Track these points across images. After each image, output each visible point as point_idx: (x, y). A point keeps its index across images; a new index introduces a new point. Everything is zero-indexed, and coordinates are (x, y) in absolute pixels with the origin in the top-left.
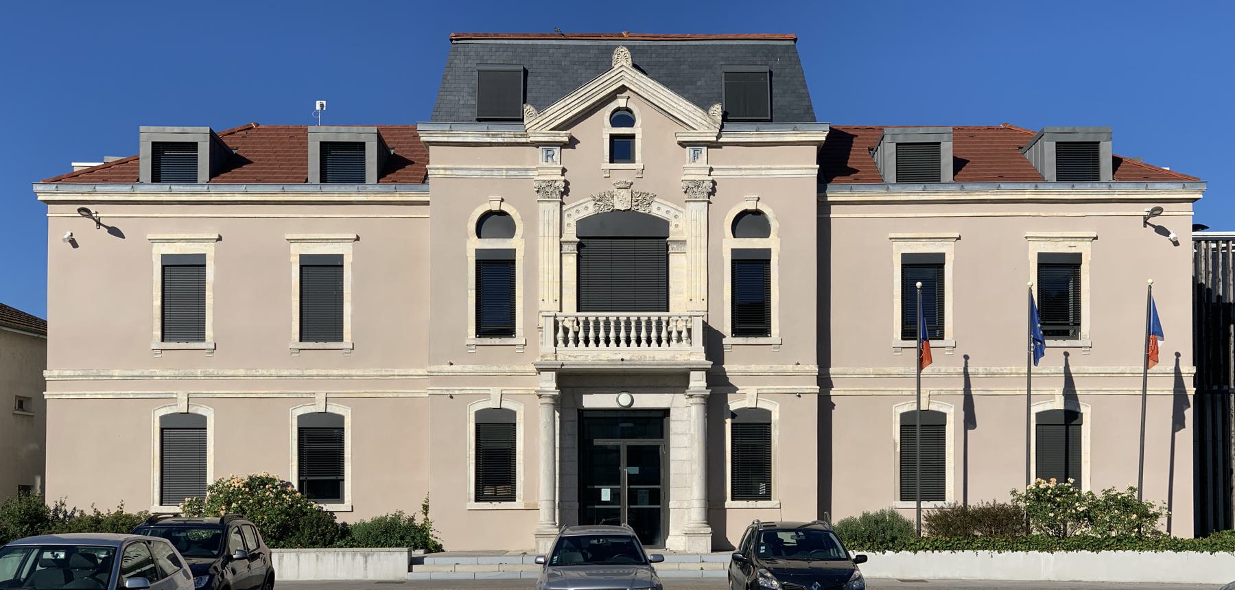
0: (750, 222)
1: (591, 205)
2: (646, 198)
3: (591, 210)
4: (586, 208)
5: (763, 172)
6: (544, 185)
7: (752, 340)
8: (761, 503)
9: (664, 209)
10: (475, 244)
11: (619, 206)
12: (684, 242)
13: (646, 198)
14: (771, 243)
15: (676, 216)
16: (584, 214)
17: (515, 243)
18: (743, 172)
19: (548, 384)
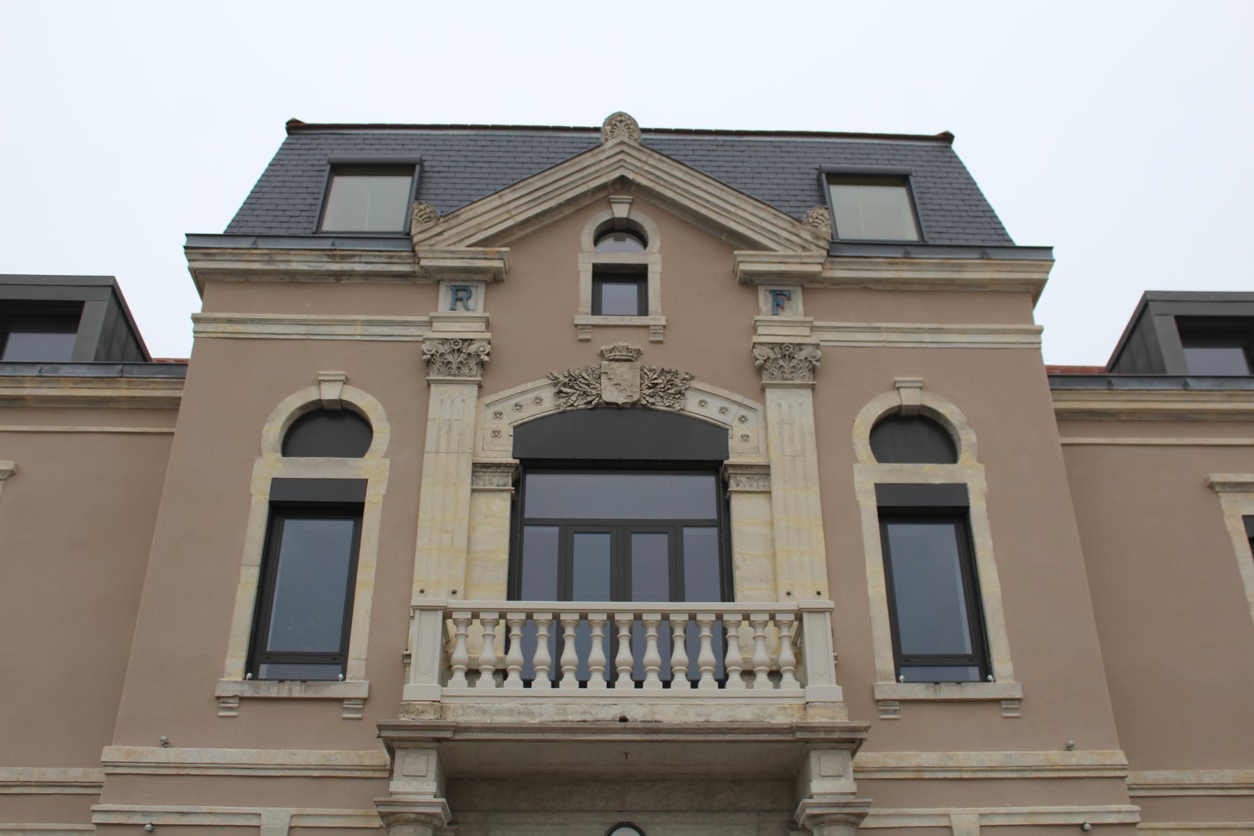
0: (913, 429)
1: (548, 395)
2: (673, 383)
3: (548, 404)
4: (539, 401)
5: (927, 337)
6: (442, 349)
7: (948, 692)
10: (272, 466)
12: (764, 471)
13: (673, 383)
14: (968, 472)
15: (743, 419)
16: (531, 412)
17: (372, 469)
18: (884, 336)
19: (413, 786)
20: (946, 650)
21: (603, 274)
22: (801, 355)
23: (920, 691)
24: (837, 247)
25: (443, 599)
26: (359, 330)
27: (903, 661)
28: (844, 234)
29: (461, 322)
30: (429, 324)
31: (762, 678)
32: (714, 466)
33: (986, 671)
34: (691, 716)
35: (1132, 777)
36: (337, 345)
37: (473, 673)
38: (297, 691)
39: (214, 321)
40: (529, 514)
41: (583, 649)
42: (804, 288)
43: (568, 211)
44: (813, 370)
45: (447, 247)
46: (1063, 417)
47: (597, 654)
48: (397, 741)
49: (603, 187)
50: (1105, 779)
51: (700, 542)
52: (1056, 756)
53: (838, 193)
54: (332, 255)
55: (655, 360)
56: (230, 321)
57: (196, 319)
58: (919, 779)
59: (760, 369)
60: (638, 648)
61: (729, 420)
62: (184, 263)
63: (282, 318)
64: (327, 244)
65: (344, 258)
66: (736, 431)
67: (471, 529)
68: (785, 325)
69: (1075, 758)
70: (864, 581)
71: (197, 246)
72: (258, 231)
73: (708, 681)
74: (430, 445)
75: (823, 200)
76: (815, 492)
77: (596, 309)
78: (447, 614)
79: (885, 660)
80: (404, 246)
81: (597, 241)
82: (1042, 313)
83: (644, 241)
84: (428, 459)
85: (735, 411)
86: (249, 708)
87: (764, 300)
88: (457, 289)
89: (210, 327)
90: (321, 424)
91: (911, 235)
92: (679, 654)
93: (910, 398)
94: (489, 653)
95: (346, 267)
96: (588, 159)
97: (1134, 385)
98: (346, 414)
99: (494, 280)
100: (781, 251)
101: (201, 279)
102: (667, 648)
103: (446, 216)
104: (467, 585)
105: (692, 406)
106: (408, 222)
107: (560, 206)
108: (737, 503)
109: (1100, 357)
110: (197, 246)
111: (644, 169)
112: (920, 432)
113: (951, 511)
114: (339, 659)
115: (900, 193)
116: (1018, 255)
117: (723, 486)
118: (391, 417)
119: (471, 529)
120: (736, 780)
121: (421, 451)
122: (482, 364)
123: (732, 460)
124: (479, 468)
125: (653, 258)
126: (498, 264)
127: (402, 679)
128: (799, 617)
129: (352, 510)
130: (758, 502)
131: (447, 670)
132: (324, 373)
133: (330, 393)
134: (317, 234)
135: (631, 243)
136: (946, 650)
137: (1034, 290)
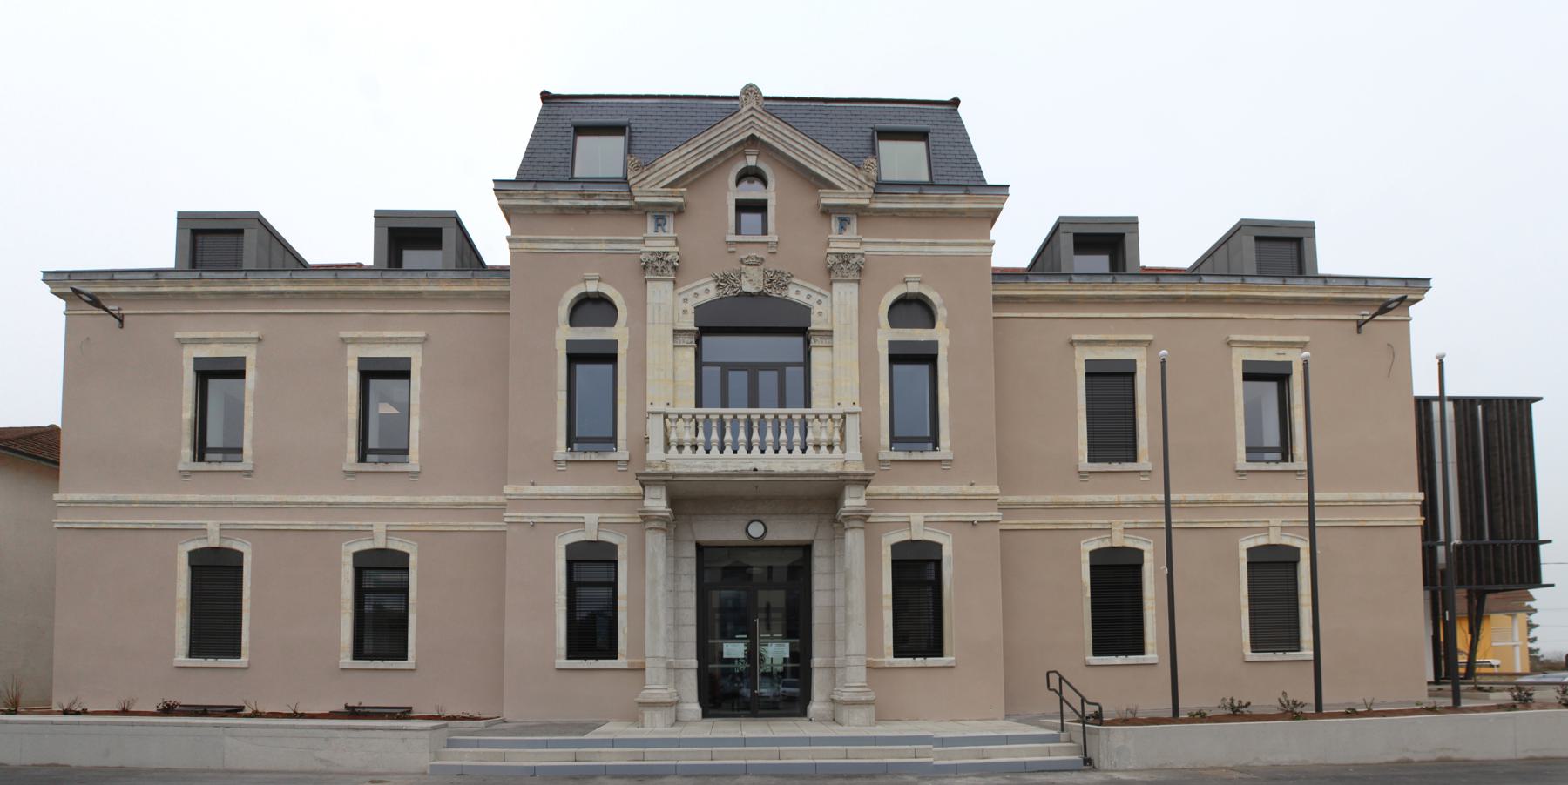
0: (913, 308)
1: (712, 287)
3: (713, 294)
4: (707, 291)
5: (926, 249)
6: (653, 258)
7: (916, 456)
8: (931, 661)
9: (804, 293)
10: (565, 334)
11: (747, 287)
13: (780, 279)
14: (940, 334)
15: (819, 302)
16: (703, 298)
17: (619, 334)
20: (916, 434)
21: (743, 207)
22: (853, 261)
23: (901, 455)
24: (881, 187)
25: (662, 408)
26: (604, 246)
27: (894, 440)
28: (885, 177)
29: (660, 240)
30: (643, 242)
31: (824, 449)
32: (803, 331)
33: (936, 445)
34: (788, 468)
35: (1001, 499)
36: (595, 255)
37: (680, 447)
38: (594, 457)
39: (520, 241)
40: (705, 359)
41: (735, 434)
42: (858, 217)
43: (720, 161)
44: (860, 270)
45: (649, 190)
46: (997, 300)
47: (742, 436)
48: (646, 481)
49: (740, 143)
50: (988, 500)
51: (794, 374)
52: (966, 489)
53: (885, 146)
54: (582, 194)
55: (772, 265)
56: (529, 241)
57: (509, 240)
58: (897, 500)
59: (830, 271)
60: (762, 433)
61: (811, 302)
62: (496, 202)
63: (560, 239)
64: (578, 187)
65: (590, 197)
66: (816, 309)
67: (675, 368)
68: (846, 241)
69: (973, 490)
70: (878, 396)
71: (501, 188)
72: (536, 177)
73: (797, 450)
74: (649, 319)
75: (874, 152)
76: (856, 344)
77: (738, 232)
78: (666, 416)
79: (885, 439)
80: (624, 188)
81: (738, 182)
82: (997, 232)
83: (765, 184)
84: (649, 327)
85: (815, 297)
86: (570, 466)
87: (835, 224)
88: (658, 218)
89: (519, 245)
90: (588, 307)
91: (925, 178)
92: (783, 436)
93: (913, 288)
94: (688, 436)
95: (592, 203)
96: (731, 122)
97: (1040, 280)
98: (601, 300)
99: (679, 211)
100: (847, 190)
101: (508, 212)
102: (777, 433)
103: (649, 165)
104: (674, 400)
105: (792, 294)
106: (625, 170)
107: (716, 157)
108: (815, 353)
109: (1024, 263)
110: (501, 188)
111: (770, 131)
112: (916, 309)
113: (927, 357)
114: (612, 440)
115: (920, 147)
116: (986, 191)
117: (807, 343)
118: (628, 302)
119: (675, 368)
120: (809, 499)
121: (645, 323)
122: (675, 268)
123: (813, 327)
124: (677, 332)
125: (770, 194)
126: (680, 200)
127: (645, 450)
128: (844, 417)
129: (612, 358)
130: (826, 351)
131: (667, 445)
132: (587, 275)
133: (592, 287)
134: (572, 180)
135: (758, 184)
136: (916, 434)
137: (993, 216)
